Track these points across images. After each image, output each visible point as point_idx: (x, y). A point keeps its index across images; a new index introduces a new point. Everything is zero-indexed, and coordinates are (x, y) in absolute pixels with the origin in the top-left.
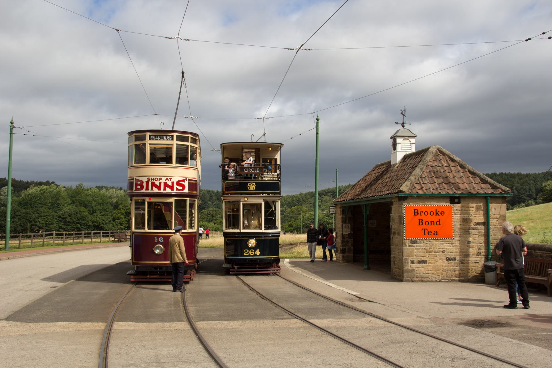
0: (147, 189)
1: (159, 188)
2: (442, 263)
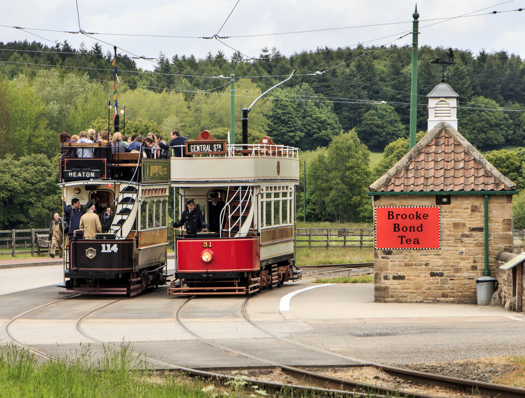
2: (423, 278)
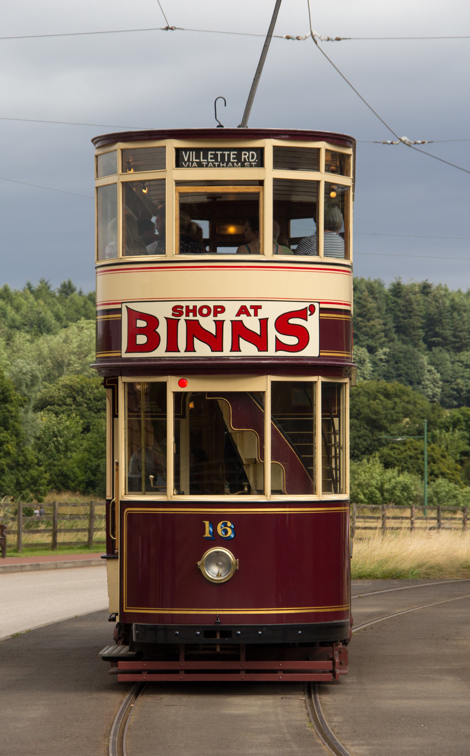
0: (172, 346)
1: (215, 342)
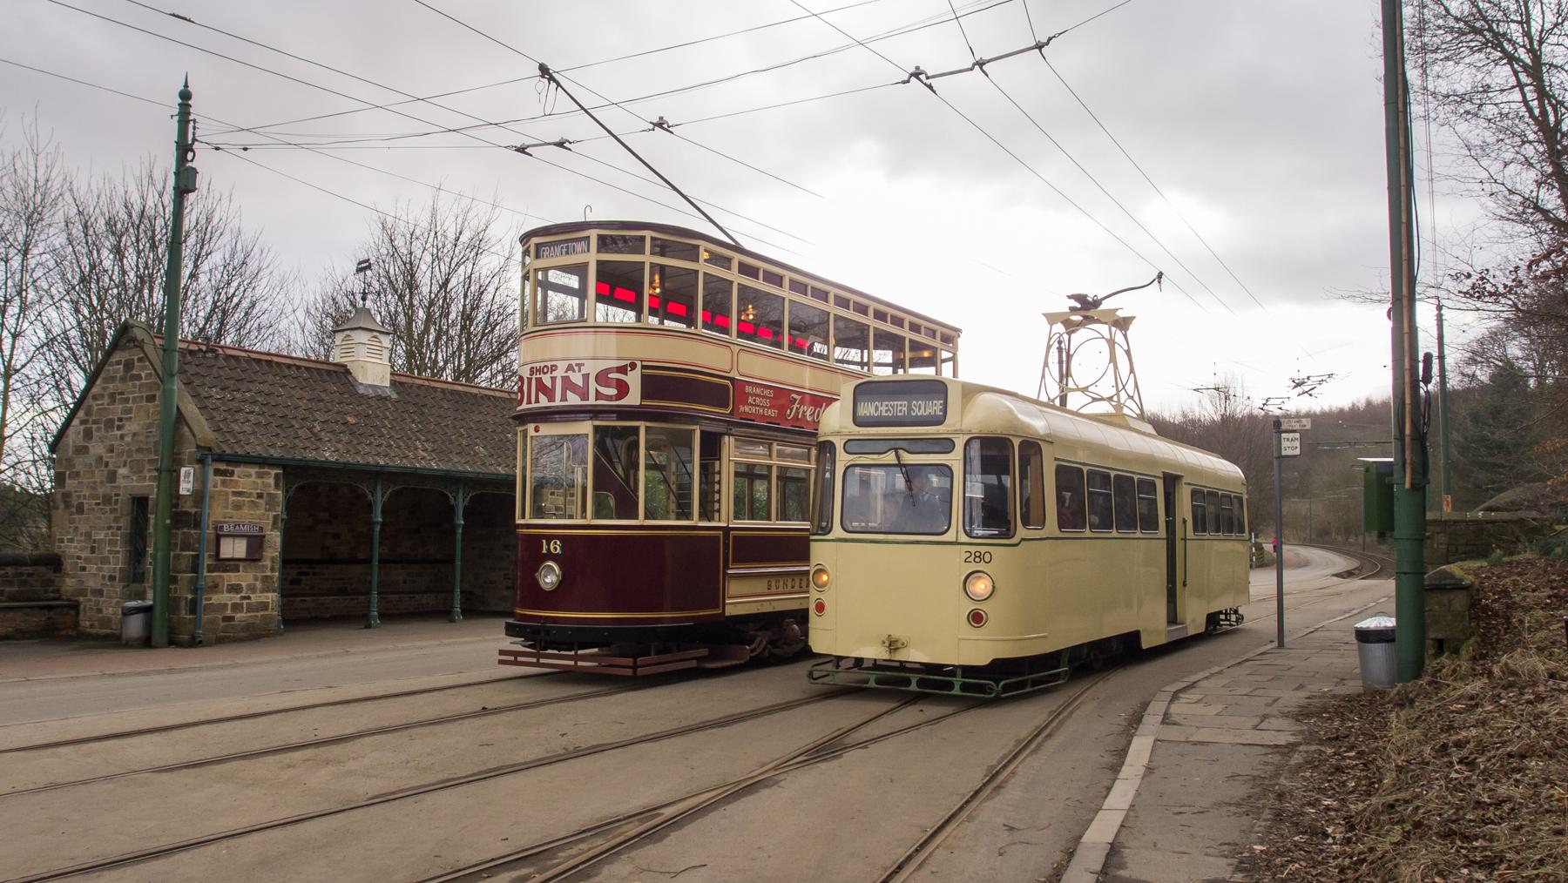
0: (529, 402)
1: (549, 393)
